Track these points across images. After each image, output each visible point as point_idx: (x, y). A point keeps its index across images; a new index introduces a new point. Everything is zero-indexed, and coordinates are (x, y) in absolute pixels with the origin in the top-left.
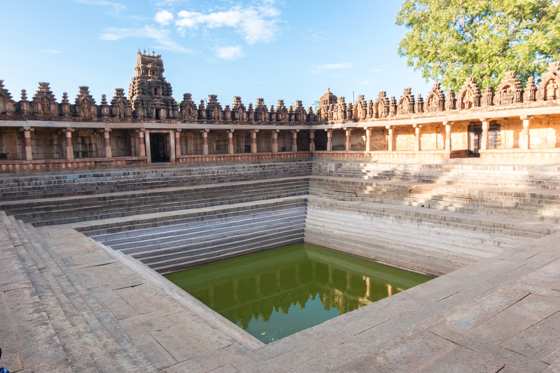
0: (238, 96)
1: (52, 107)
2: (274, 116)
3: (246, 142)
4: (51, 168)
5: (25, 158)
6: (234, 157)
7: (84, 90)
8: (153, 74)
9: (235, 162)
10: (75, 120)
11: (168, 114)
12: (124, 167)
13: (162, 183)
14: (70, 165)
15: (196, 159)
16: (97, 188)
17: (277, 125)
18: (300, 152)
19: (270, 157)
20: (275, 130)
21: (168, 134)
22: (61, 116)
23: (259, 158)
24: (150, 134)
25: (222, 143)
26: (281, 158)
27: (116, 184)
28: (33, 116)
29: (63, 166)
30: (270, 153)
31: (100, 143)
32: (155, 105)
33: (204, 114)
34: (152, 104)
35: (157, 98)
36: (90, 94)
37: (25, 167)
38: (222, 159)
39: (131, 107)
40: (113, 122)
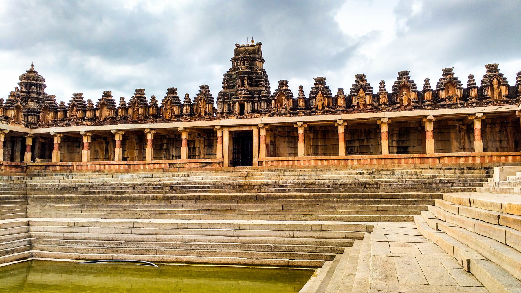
0: (360, 73)
1: (140, 110)
2: (428, 96)
3: (398, 142)
4: (131, 169)
5: (113, 160)
6: (345, 160)
7: (172, 91)
8: (244, 64)
9: (346, 167)
10: (156, 122)
11: (253, 108)
12: (197, 170)
13: (204, 187)
14: (147, 167)
15: (286, 163)
16: (134, 188)
17: (434, 108)
18: (489, 153)
19: (417, 161)
20: (425, 117)
21: (251, 132)
22: (145, 119)
23: (393, 164)
24: (230, 133)
25: (357, 144)
26: (443, 164)
27: (156, 185)
28: (124, 120)
29: (142, 167)
30: (416, 155)
31: (203, 147)
32: (238, 98)
33: (301, 103)
34: (235, 98)
35: (241, 90)
36: (177, 95)
37: (112, 167)
38: (326, 163)
39: (213, 104)
40: (191, 121)
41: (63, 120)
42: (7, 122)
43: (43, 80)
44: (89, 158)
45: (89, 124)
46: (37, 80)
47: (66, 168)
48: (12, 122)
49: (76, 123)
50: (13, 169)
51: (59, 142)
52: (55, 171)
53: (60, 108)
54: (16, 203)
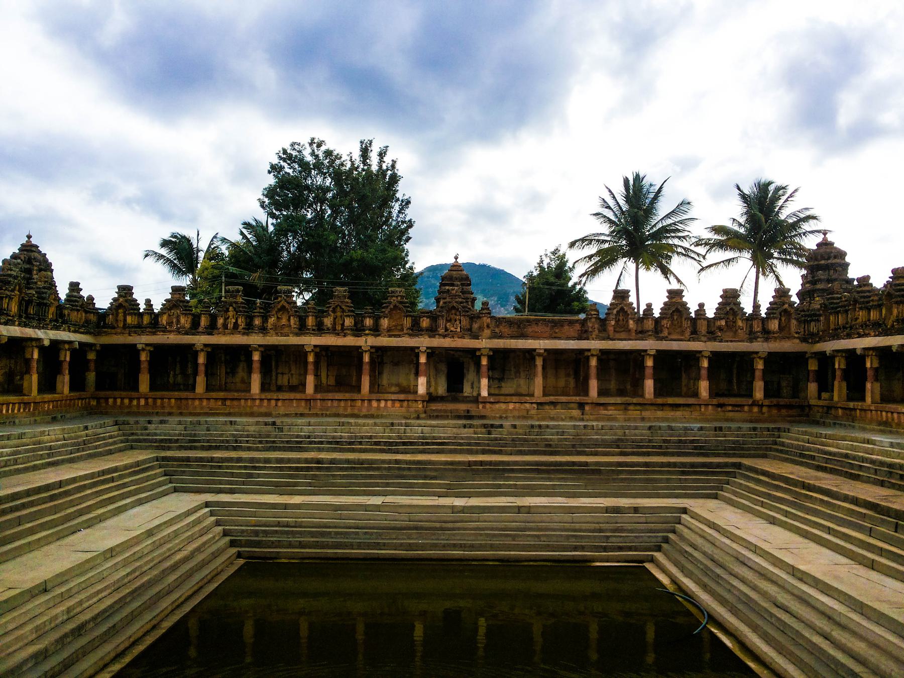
41: (845, 328)
42: (767, 340)
43: (842, 254)
44: (878, 397)
45: (873, 334)
46: (829, 258)
47: (848, 412)
48: (776, 338)
49: (858, 333)
50: (784, 412)
51: (843, 366)
52: (836, 417)
53: (841, 307)
54: (713, 473)
